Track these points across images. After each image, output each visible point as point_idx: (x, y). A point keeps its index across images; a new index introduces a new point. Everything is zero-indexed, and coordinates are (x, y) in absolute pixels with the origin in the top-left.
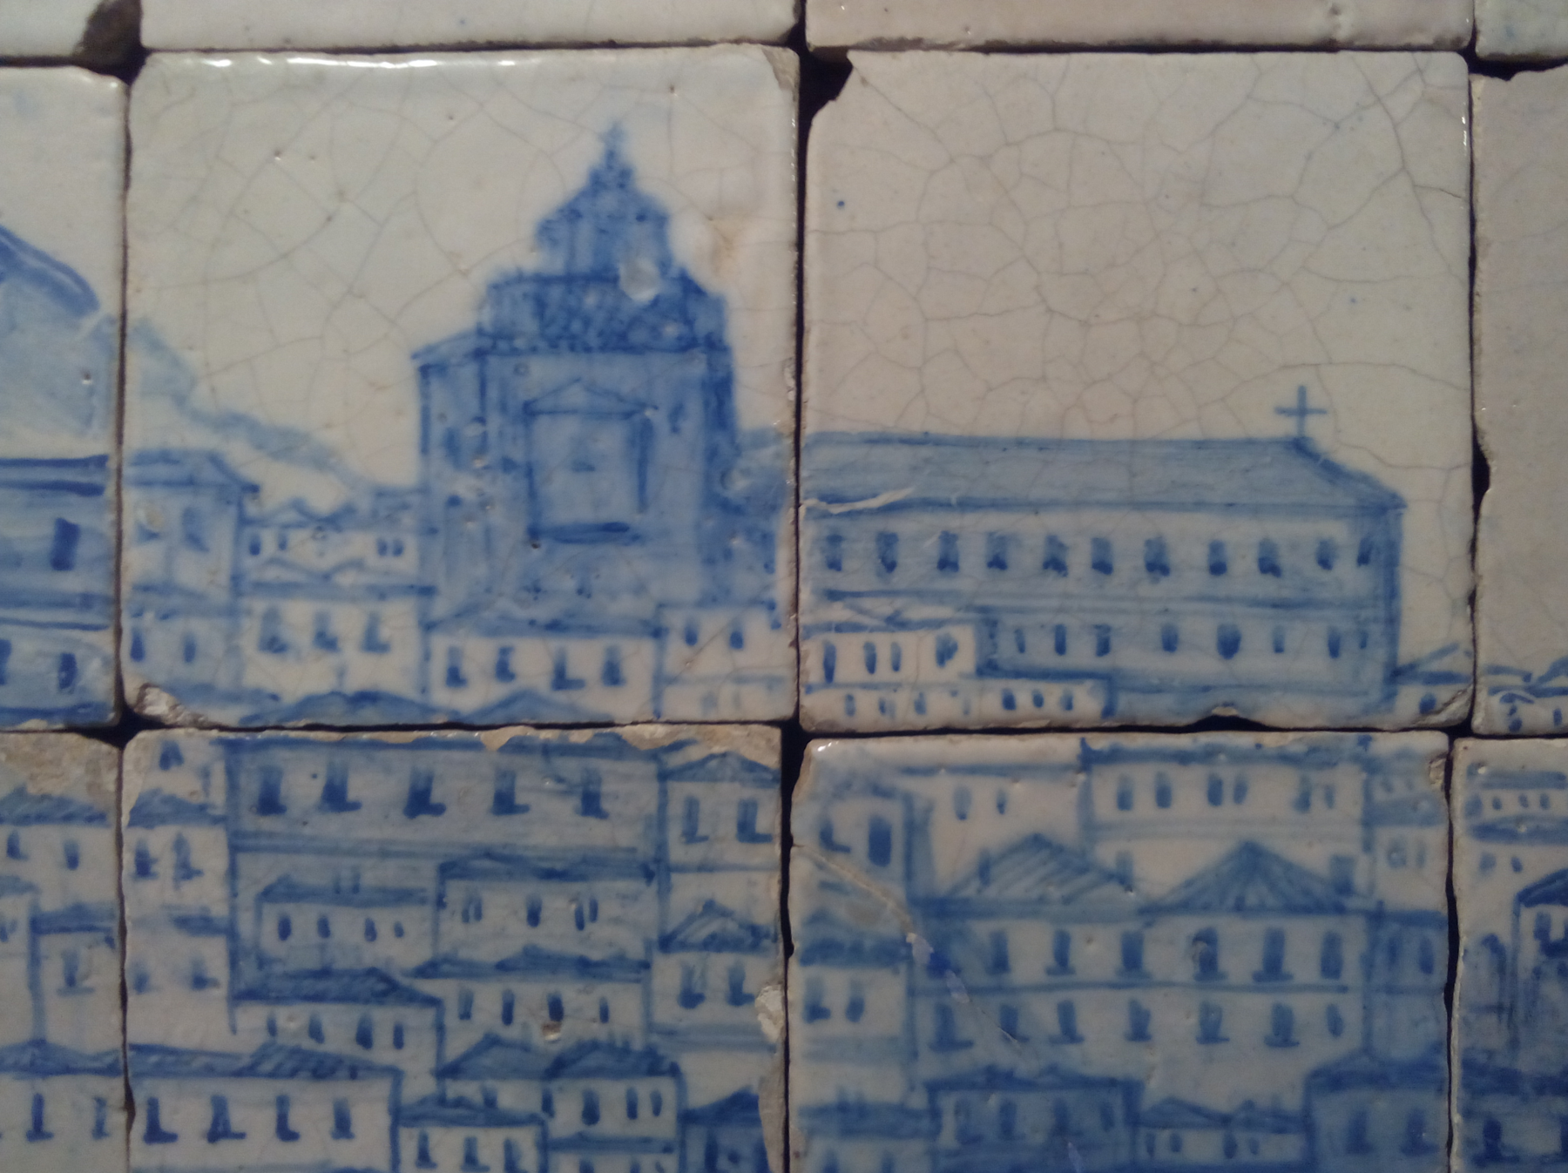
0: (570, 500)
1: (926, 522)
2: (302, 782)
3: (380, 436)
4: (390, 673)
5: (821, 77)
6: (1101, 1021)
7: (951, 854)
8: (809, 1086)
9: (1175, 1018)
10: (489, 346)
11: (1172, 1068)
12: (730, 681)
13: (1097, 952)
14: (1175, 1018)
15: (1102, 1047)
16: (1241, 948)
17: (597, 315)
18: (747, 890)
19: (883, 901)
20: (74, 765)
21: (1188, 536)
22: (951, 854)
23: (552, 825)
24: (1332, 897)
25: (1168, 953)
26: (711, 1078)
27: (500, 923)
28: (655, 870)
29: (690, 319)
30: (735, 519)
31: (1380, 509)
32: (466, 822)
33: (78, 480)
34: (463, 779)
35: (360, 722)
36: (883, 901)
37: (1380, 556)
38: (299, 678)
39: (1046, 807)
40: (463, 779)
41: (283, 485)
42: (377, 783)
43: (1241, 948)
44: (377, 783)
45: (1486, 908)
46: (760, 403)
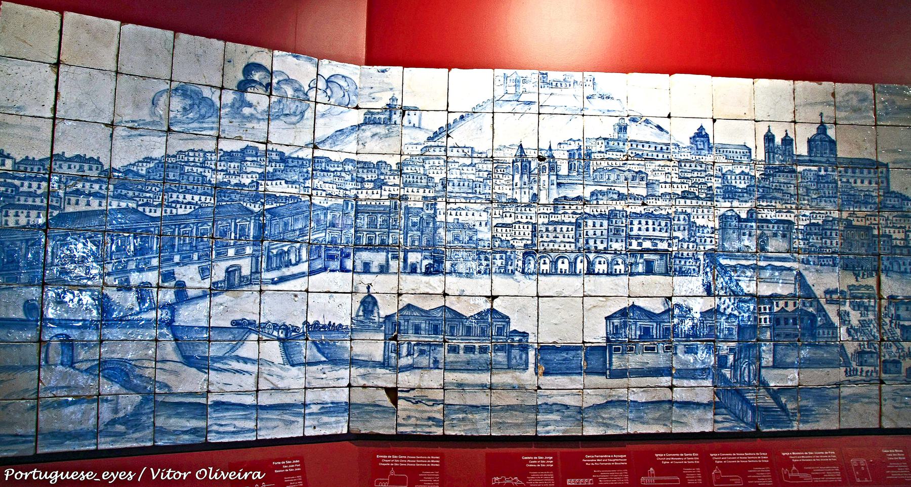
0: (699, 147)
1: (722, 149)
2: (683, 164)
3: (687, 143)
4: (689, 158)
5: (714, 121)
6: (734, 182)
7: (724, 171)
8: (716, 185)
9: (738, 182)
10: (694, 137)
11: (738, 185)
12: (709, 159)
13: (733, 177)
14: (738, 182)
15: (734, 184)
16: (742, 177)
17: (701, 135)
18: (711, 173)
19: (720, 174)
20: (668, 163)
21: (738, 151)
22: (724, 171)
23: (699, 168)
24: (748, 174)
25: (738, 177)
26: (709, 185)
27: (695, 174)
28: (705, 171)
29: (707, 135)
30: (710, 149)
31: (750, 150)
32: (693, 168)
33: (668, 144)
34: (693, 165)
35: (686, 161)
36: (720, 174)
37: (750, 152)
38: (682, 158)
39: (730, 168)
40: (693, 165)
41: (681, 146)
42: (688, 165)
43: (742, 177)
44: (688, 165)
45: (757, 175)
46: (711, 141)
